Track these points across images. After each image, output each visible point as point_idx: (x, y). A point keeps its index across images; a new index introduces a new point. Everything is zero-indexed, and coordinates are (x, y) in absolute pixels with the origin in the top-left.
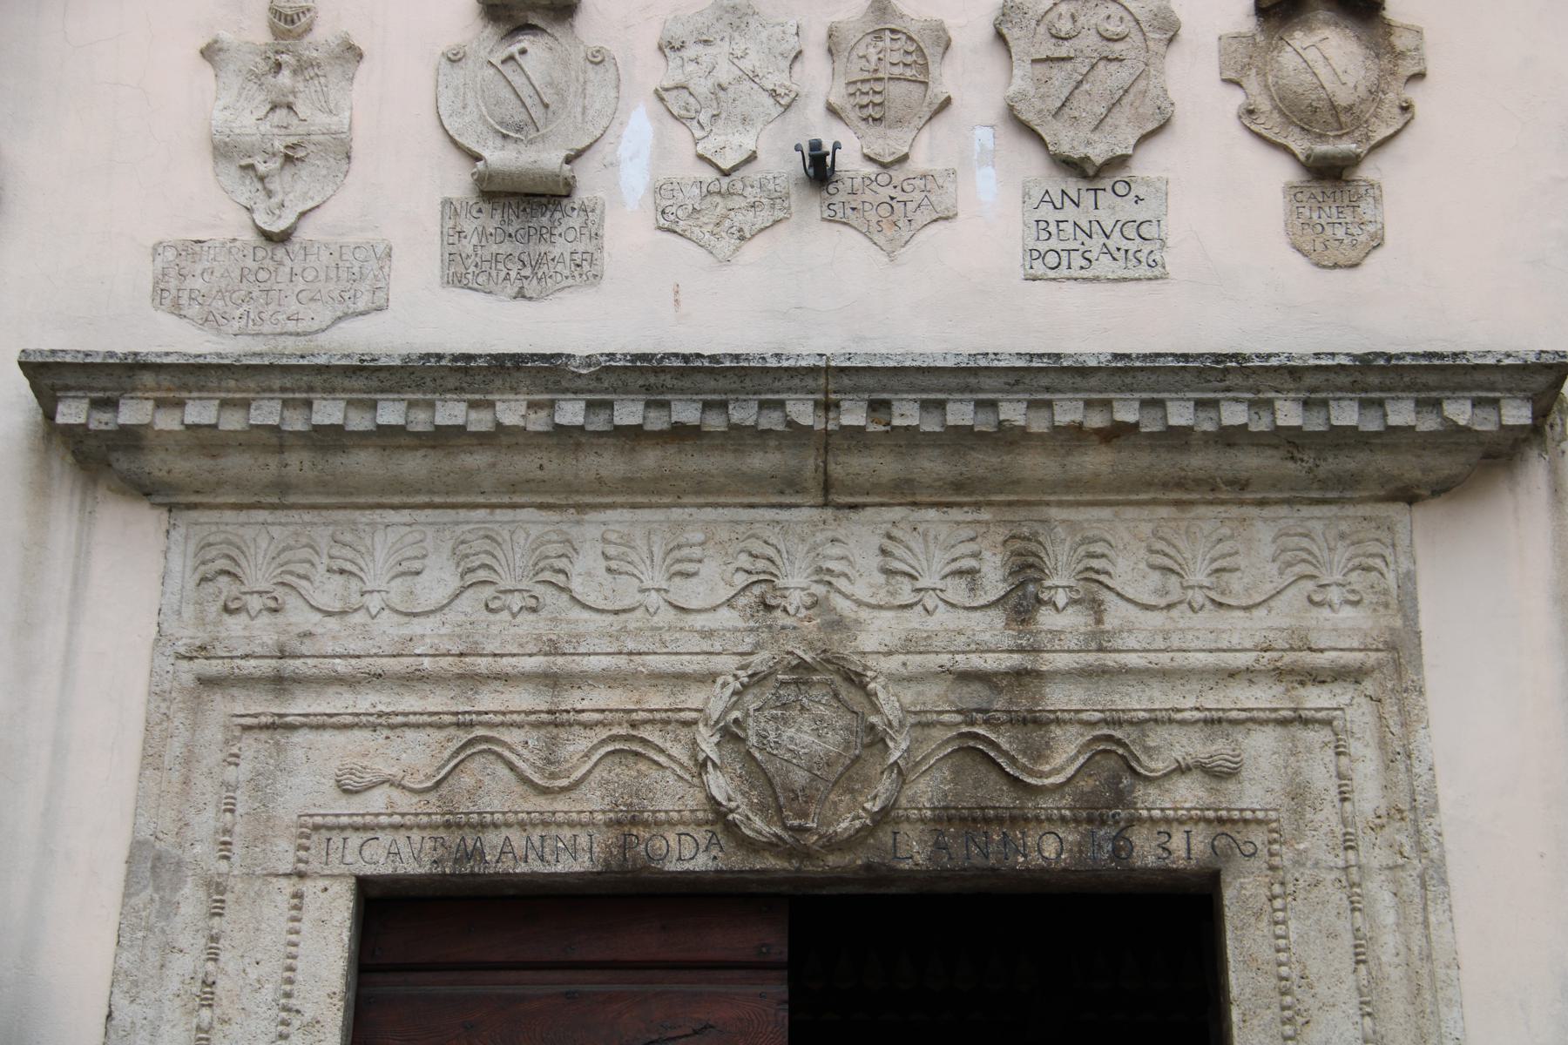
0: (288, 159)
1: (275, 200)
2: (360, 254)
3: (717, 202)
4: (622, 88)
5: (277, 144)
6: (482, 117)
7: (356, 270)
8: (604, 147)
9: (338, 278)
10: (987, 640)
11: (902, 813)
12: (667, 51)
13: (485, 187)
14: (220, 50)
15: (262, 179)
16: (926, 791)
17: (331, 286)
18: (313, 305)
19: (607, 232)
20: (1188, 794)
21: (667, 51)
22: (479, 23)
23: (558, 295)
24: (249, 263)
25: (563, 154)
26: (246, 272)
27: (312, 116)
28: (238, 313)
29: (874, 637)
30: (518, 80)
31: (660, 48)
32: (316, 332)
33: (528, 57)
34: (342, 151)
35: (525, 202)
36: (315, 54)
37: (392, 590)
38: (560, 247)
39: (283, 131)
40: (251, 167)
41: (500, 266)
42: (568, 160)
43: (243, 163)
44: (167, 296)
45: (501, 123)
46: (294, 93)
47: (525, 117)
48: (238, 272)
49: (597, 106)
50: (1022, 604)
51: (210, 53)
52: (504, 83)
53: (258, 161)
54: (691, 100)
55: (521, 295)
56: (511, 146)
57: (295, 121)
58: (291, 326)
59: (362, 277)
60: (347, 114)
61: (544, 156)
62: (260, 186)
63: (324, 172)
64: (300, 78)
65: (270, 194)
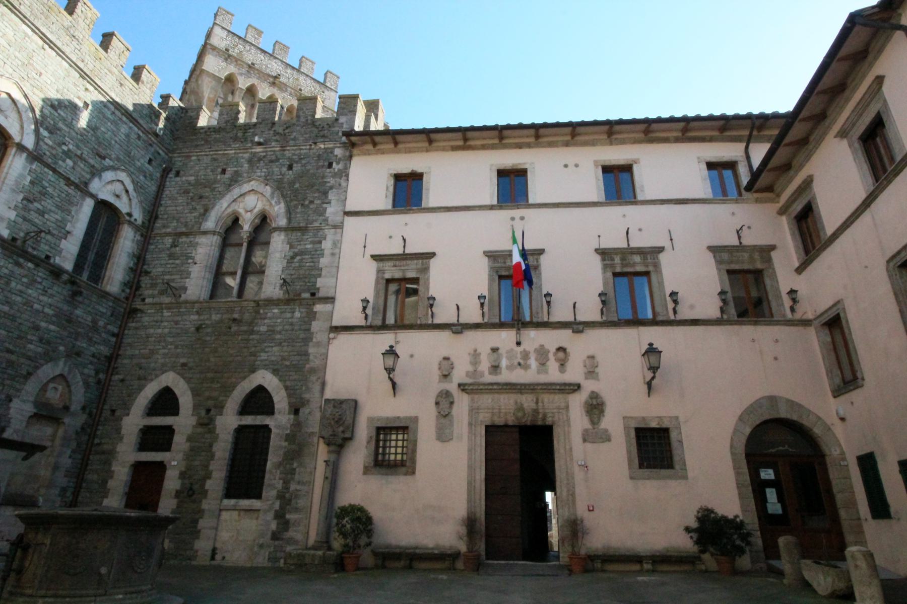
3: (510, 368)
10: (533, 406)
11: (527, 420)
16: (530, 418)
20: (550, 419)
29: (526, 405)
35: (495, 368)
37: (486, 400)
44: (467, 376)
50: (537, 403)
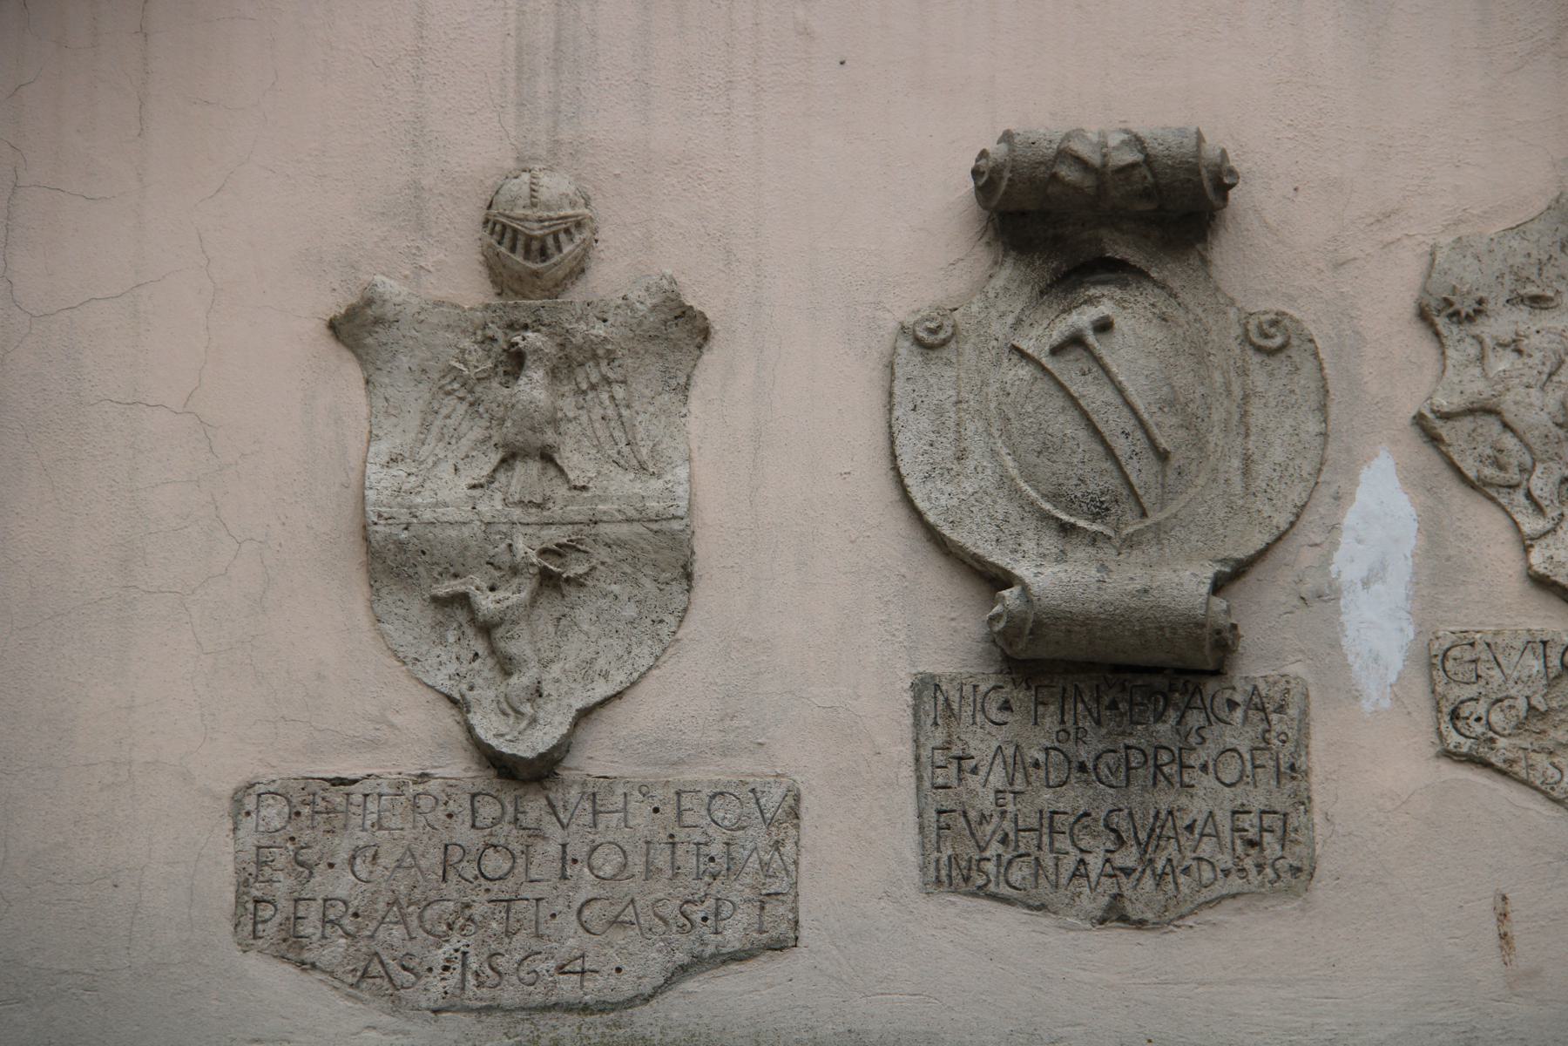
0: (549, 582)
1: (521, 681)
2: (726, 812)
4: (1334, 410)
5: (520, 545)
6: (1004, 480)
7: (716, 849)
8: (1300, 554)
9: (676, 870)
12: (1441, 322)
13: (1021, 649)
14: (378, 321)
15: (487, 629)
17: (660, 888)
18: (618, 937)
19: (1319, 759)
21: (1441, 322)
22: (982, 257)
23: (1208, 915)
24: (463, 833)
25: (1209, 572)
26: (456, 854)
27: (602, 482)
28: (439, 956)
30: (1094, 395)
31: (1424, 315)
32: (630, 1003)
33: (1116, 339)
34: (670, 558)
36: (600, 330)
38: (1206, 799)
39: (534, 515)
40: (463, 600)
41: (1063, 843)
42: (1219, 585)
43: (446, 588)
45: (1054, 497)
46: (554, 422)
47: (1113, 482)
48: (435, 856)
49: (1278, 454)
51: (355, 328)
52: (1059, 401)
53: (474, 584)
54: (1509, 441)
55: (1115, 914)
56: (1081, 553)
57: (562, 491)
58: (568, 988)
59: (733, 869)
60: (682, 472)
61: (1164, 576)
62: (480, 646)
63: (630, 611)
64: (567, 388)
65: (506, 666)
